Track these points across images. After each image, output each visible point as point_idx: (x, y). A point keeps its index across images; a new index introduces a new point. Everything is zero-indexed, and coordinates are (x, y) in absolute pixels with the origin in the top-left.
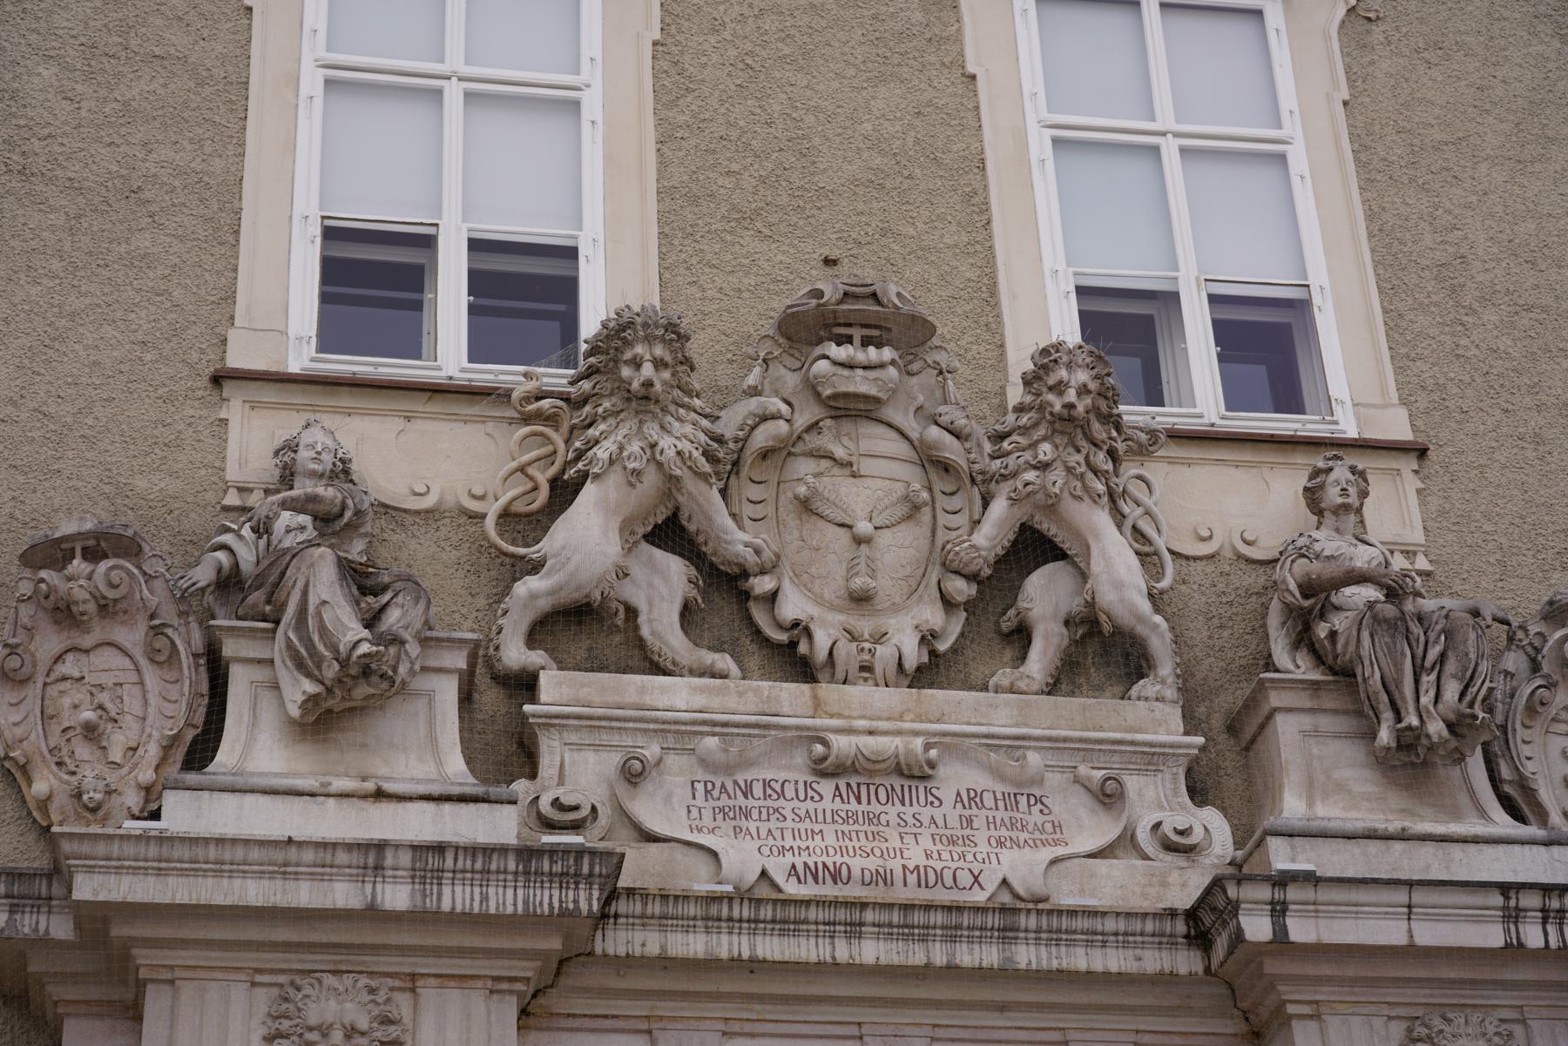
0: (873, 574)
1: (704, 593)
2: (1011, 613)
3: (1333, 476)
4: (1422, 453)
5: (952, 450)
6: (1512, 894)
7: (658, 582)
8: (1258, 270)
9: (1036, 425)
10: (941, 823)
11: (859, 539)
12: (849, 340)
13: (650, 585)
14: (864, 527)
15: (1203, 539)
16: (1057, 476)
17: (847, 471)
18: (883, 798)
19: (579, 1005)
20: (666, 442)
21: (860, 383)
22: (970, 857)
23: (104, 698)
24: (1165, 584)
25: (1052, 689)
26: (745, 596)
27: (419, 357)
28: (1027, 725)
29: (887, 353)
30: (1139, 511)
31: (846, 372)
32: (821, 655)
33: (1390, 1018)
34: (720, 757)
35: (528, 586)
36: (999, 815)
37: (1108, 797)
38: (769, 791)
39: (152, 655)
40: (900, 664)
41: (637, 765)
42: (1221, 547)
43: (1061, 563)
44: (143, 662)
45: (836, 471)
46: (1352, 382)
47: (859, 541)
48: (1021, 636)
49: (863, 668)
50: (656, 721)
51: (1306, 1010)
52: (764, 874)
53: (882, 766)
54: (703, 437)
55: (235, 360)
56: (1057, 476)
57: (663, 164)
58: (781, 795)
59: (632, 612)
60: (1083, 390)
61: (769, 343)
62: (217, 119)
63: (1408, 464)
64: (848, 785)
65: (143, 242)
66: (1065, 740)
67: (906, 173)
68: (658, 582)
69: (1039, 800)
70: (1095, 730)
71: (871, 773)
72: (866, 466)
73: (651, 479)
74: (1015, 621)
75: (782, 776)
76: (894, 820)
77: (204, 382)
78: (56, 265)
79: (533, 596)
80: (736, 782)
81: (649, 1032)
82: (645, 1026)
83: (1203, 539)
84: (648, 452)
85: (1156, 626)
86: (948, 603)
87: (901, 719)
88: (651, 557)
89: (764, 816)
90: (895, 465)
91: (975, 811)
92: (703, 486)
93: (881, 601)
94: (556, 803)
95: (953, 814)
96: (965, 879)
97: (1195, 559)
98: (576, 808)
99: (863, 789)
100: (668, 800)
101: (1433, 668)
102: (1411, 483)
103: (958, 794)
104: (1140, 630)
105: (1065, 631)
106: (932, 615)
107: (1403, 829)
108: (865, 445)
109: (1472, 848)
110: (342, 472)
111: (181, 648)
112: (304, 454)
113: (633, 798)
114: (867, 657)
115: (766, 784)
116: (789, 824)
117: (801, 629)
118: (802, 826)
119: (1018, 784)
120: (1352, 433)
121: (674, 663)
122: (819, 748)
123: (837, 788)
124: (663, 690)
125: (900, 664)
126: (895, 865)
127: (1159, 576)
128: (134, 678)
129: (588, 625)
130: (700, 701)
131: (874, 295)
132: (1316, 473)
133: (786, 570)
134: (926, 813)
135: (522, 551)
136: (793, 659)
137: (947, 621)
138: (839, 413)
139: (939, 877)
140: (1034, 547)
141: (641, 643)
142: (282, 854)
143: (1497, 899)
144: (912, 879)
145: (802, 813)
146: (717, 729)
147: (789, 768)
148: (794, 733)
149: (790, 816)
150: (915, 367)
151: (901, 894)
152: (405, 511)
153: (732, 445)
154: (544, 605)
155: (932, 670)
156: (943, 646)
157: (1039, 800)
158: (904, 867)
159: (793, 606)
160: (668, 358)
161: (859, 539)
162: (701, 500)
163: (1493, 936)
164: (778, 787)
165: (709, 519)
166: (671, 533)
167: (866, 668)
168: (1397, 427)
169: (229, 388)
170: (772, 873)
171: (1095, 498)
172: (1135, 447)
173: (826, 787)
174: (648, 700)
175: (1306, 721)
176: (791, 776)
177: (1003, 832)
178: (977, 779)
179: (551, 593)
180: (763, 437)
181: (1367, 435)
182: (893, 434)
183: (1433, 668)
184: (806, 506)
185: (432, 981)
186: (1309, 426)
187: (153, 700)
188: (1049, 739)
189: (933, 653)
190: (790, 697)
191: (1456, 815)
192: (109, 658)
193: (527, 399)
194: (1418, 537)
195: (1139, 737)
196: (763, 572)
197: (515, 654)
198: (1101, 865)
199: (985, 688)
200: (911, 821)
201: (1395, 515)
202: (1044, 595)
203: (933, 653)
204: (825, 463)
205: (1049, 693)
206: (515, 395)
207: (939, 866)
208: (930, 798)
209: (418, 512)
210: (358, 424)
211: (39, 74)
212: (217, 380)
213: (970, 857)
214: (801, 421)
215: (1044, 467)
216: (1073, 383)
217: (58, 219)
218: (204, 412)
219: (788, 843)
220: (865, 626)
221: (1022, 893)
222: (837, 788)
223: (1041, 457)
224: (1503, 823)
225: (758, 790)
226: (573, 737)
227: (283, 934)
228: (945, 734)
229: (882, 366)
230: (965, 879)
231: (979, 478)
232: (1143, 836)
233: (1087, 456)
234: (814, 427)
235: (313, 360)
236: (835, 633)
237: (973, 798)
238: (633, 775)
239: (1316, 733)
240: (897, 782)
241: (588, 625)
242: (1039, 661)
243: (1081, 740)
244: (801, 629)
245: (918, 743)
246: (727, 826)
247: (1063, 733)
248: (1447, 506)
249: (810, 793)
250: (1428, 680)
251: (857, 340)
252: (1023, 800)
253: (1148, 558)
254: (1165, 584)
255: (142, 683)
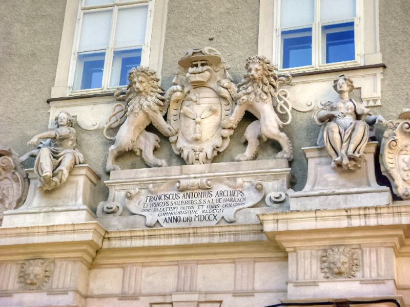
0: (201, 132)
1: (160, 144)
2: (243, 138)
3: (339, 82)
4: (384, 67)
5: (225, 93)
6: (349, 211)
7: (147, 142)
8: (338, 16)
9: (249, 82)
10: (211, 201)
11: (204, 121)
12: (196, 66)
13: (146, 143)
14: (198, 119)
15: (309, 106)
16: (252, 96)
17: (195, 103)
18: (196, 196)
19: (105, 261)
20: (145, 104)
21: (198, 78)
22: (215, 211)
23: (4, 192)
24: (288, 122)
25: (255, 158)
26: (170, 143)
27: (90, 88)
28: (237, 171)
29: (206, 67)
30: (282, 102)
31: (193, 75)
32: (185, 158)
33: (318, 250)
34: (153, 190)
35: (113, 147)
36: (227, 198)
37: (259, 189)
38: (166, 197)
39: (14, 179)
40: (207, 158)
41: (129, 194)
42: (314, 107)
43: (255, 122)
44: (13, 182)
45: (194, 104)
46: (365, 47)
47: (197, 123)
48: (246, 143)
49: (196, 159)
50: (138, 181)
51: (292, 249)
52: (158, 221)
53: (195, 187)
54: (157, 100)
55: (53, 96)
56: (252, 96)
57: (169, 19)
58: (169, 198)
59: (141, 151)
60: (257, 70)
61: (179, 69)
62: (56, 30)
63: (381, 70)
64: (187, 193)
65: (35, 67)
66: (249, 173)
67: (237, 7)
68: (147, 142)
69: (241, 192)
70: (259, 169)
71: (193, 190)
72: (201, 101)
73: (141, 116)
74: (244, 141)
75: (169, 193)
76: (198, 202)
77: (47, 104)
78: (15, 78)
79: (112, 150)
80: (157, 196)
81: (123, 267)
82: (121, 266)
83: (309, 106)
84: (140, 106)
85: (280, 137)
86: (223, 138)
87: (204, 173)
88: (146, 135)
89: (163, 204)
90: (210, 99)
91: (221, 197)
92: (155, 113)
93: (204, 138)
94: (107, 208)
95: (214, 198)
96: (212, 217)
97: (306, 112)
98: (111, 208)
99: (191, 194)
100: (139, 203)
101: (346, 141)
102: (380, 77)
103: (217, 193)
104: (276, 138)
105: (258, 141)
106: (218, 142)
107: (333, 192)
108: (202, 95)
109: (355, 195)
110: (72, 123)
111: (19, 178)
112: (59, 120)
113: (129, 203)
114: (197, 156)
115: (165, 196)
116: (169, 206)
117: (181, 150)
118: (172, 207)
119: (235, 188)
120: (362, 65)
121: (150, 164)
122: (178, 184)
123: (184, 195)
124: (142, 172)
125: (207, 158)
126: (193, 216)
127: (287, 120)
128: (11, 186)
129: (127, 156)
130: (150, 174)
131: (201, 52)
132: (335, 81)
133: (180, 135)
134: (207, 199)
135: (112, 138)
136: (182, 160)
137: (223, 143)
138: (195, 87)
139: (205, 218)
140: (249, 117)
141: (142, 159)
142: (29, 231)
143: (344, 213)
144: (197, 219)
145: (173, 203)
146: (154, 182)
147: (173, 190)
148: (174, 180)
149: (170, 203)
150: (218, 69)
151: (194, 224)
152: (90, 130)
153: (168, 101)
154: (115, 152)
155: (218, 156)
156: (221, 150)
157: (241, 192)
158: (195, 216)
159: (181, 143)
160: (143, 79)
161: (204, 121)
162: (155, 118)
163: (344, 223)
164: (168, 196)
165: (158, 123)
166: (151, 128)
167: (198, 159)
168: (378, 60)
169: (51, 103)
170: (159, 221)
171: (263, 100)
172: (282, 82)
173: (181, 195)
174: (137, 176)
175: (317, 160)
176: (172, 193)
177: (228, 202)
178: (223, 188)
179: (116, 149)
180: (174, 98)
181: (366, 64)
182: (212, 90)
183: (346, 141)
184: (186, 116)
185: (58, 260)
186: (347, 65)
187: (15, 191)
188: (245, 174)
189: (218, 153)
190: (175, 171)
191: (359, 185)
192: (6, 181)
193: (118, 95)
194: (379, 94)
195: (271, 170)
196: (173, 135)
197: (110, 165)
198: (252, 210)
199: (233, 160)
200: (202, 201)
201: (370, 87)
202: (251, 132)
203: (218, 153)
204: (191, 102)
205: (253, 160)
206: (115, 94)
207: (205, 214)
208: (209, 195)
209: (93, 130)
210: (82, 108)
211: (16, 27)
212: (48, 102)
213: (215, 211)
214: (186, 90)
215: (249, 94)
216: (253, 68)
217: (16, 65)
218: (45, 111)
219: (168, 211)
220: (197, 147)
221: (227, 220)
222: (184, 195)
223: (247, 91)
224: (375, 185)
225: (163, 197)
226: (118, 188)
227: (21, 251)
228: (215, 176)
229: (203, 72)
230: (212, 217)
231: (234, 99)
232: (267, 200)
233: (262, 89)
234: (189, 92)
235: (72, 92)
236: (190, 150)
237: (222, 193)
238: (129, 197)
239: (320, 164)
240: (200, 191)
241: (127, 156)
242: (249, 151)
243: (254, 173)
244: (181, 150)
245: (204, 180)
246: (152, 208)
247: (248, 172)
248: (391, 83)
249: (177, 197)
250: (345, 144)
251: (199, 65)
252: (236, 193)
253: (283, 117)
254: (288, 122)
255: (12, 187)
